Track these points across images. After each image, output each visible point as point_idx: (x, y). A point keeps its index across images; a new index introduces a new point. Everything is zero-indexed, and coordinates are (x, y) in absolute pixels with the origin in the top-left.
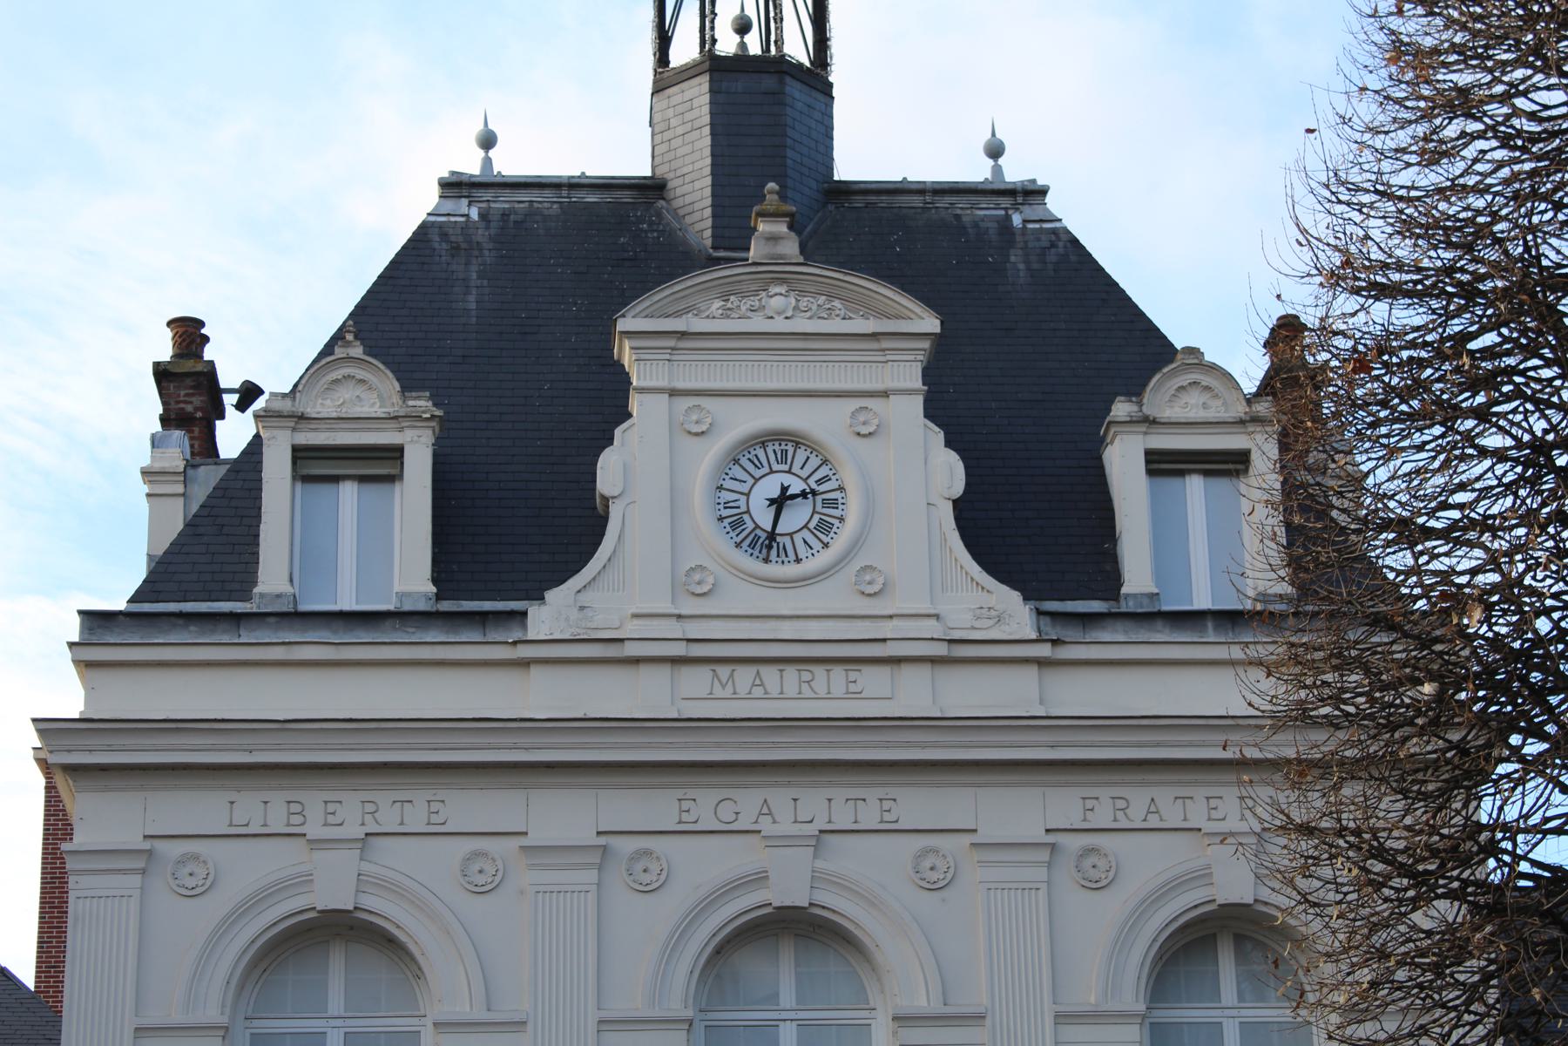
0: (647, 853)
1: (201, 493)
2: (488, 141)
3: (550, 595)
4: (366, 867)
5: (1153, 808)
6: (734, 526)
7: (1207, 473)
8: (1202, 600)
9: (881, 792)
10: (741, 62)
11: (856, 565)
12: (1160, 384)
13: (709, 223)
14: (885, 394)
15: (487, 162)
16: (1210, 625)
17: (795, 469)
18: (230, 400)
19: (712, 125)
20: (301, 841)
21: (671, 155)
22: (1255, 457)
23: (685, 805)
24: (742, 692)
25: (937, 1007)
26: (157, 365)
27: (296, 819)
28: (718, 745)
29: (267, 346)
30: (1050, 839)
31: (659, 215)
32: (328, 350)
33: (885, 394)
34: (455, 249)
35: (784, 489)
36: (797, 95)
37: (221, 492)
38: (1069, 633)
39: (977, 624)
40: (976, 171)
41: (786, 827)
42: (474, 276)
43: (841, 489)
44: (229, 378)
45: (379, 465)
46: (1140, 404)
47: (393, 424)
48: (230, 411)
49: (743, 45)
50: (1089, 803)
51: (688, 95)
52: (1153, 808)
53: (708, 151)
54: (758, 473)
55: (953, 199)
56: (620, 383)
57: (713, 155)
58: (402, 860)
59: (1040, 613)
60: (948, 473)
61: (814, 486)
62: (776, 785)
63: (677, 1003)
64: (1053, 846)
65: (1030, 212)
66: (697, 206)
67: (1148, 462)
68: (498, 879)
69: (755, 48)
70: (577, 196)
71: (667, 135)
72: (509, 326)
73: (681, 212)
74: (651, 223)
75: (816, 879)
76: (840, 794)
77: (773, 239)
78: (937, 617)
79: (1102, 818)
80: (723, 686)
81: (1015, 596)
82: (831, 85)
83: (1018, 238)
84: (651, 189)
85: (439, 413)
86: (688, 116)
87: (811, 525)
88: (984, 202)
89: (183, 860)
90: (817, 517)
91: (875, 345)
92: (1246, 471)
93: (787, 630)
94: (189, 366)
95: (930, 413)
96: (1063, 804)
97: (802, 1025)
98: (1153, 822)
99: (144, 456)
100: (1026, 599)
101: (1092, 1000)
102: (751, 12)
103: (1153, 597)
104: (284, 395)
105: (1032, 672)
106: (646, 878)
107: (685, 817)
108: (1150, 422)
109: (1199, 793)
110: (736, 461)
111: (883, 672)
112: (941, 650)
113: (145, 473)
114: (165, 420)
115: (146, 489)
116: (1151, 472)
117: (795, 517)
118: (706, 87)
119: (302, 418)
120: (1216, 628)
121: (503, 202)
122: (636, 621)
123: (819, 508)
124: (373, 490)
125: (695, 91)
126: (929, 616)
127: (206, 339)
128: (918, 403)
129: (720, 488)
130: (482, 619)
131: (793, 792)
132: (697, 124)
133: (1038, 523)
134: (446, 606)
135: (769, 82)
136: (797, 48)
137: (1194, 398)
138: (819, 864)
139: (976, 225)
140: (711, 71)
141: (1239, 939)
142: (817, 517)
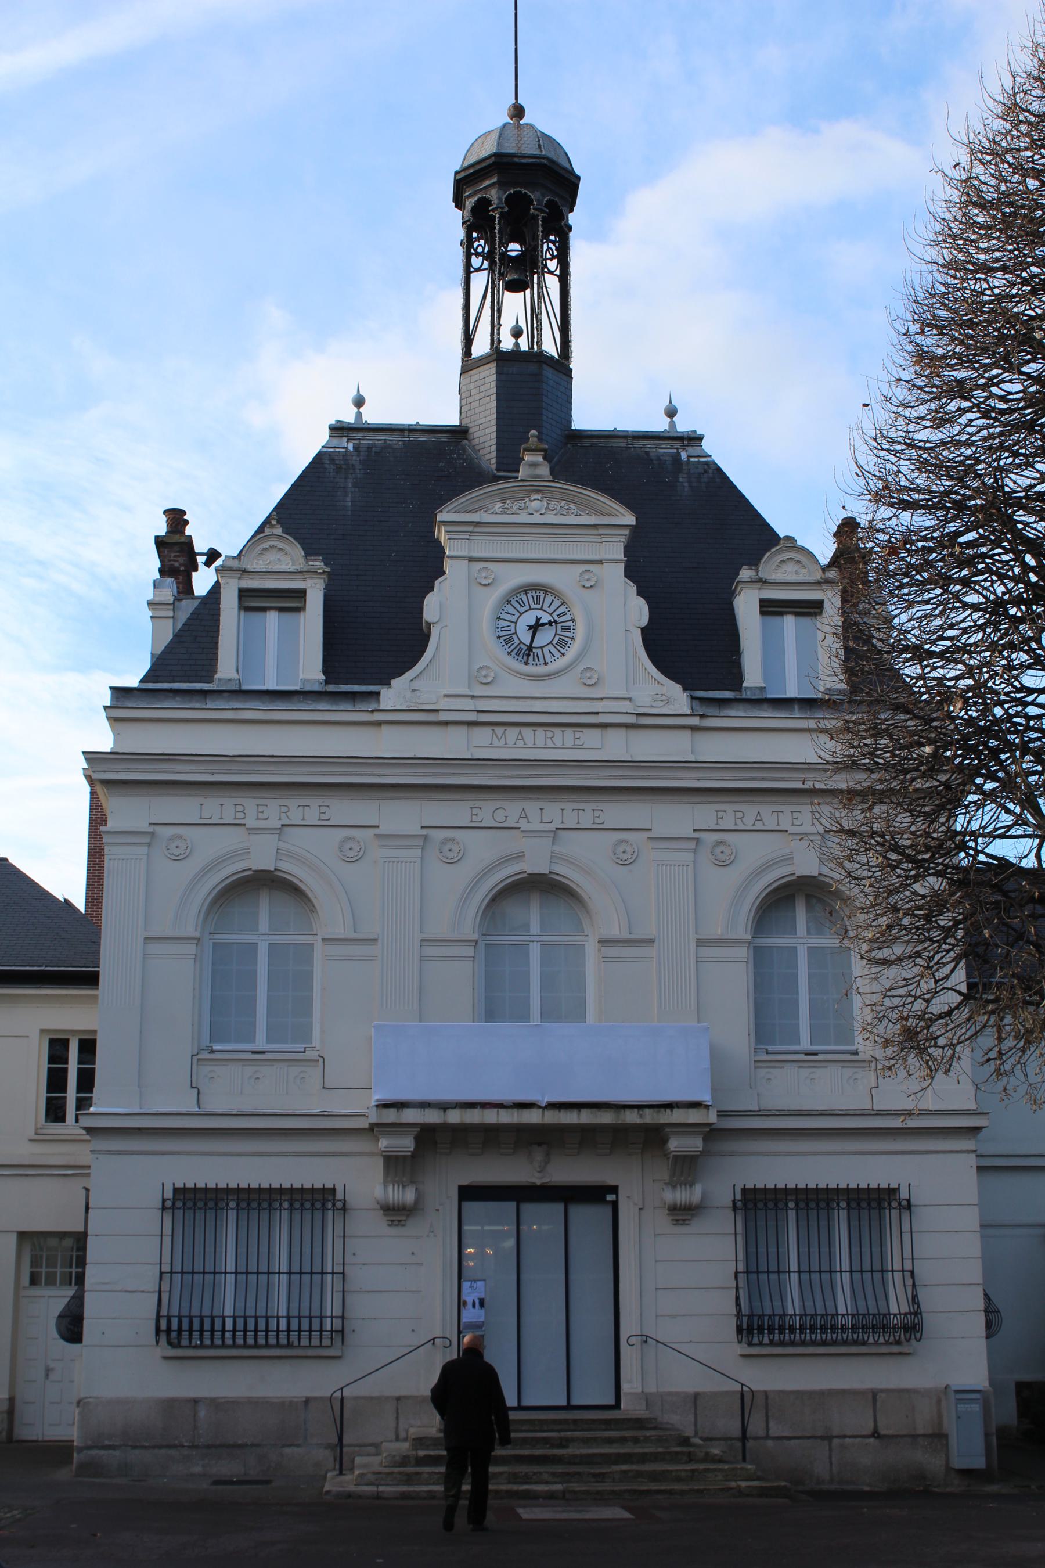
0: (451, 840)
1: (183, 616)
2: (359, 402)
3: (394, 682)
4: (281, 845)
5: (759, 818)
6: (507, 642)
7: (797, 614)
8: (792, 692)
9: (594, 805)
10: (516, 354)
11: (581, 667)
12: (769, 558)
13: (494, 454)
14: (601, 562)
15: (359, 415)
16: (796, 707)
17: (545, 608)
18: (201, 559)
19: (497, 394)
20: (242, 828)
21: (472, 412)
22: (826, 605)
23: (475, 811)
24: (510, 743)
25: (626, 936)
26: (157, 538)
27: (240, 815)
28: (496, 775)
29: (224, 528)
30: (696, 835)
31: (464, 450)
32: (260, 530)
33: (601, 562)
34: (339, 469)
35: (538, 620)
36: (550, 376)
37: (195, 615)
38: (710, 711)
39: (654, 704)
40: (659, 424)
41: (536, 826)
42: (350, 485)
43: (573, 620)
44: (200, 546)
45: (291, 601)
46: (757, 571)
47: (300, 576)
48: (201, 567)
49: (517, 344)
50: (720, 814)
51: (482, 375)
52: (759, 818)
53: (494, 410)
54: (522, 610)
55: (645, 442)
56: (439, 552)
57: (497, 413)
58: (304, 842)
59: (693, 698)
60: (639, 611)
61: (556, 618)
63: (469, 929)
64: (698, 840)
65: (692, 451)
66: (487, 444)
67: (761, 606)
68: (361, 854)
69: (524, 346)
70: (413, 437)
71: (469, 400)
72: (371, 518)
73: (477, 448)
74: (459, 454)
75: (554, 857)
76: (569, 806)
77: (534, 465)
78: (630, 699)
79: (728, 823)
81: (678, 688)
82: (571, 370)
83: (684, 467)
84: (459, 433)
85: (328, 569)
86: (483, 388)
87: (554, 642)
88: (664, 444)
89: (172, 839)
90: (557, 637)
91: (595, 532)
92: (821, 613)
93: (538, 706)
94: (176, 538)
95: (629, 574)
96: (704, 814)
97: (544, 944)
98: (759, 826)
99: (149, 594)
100: (685, 689)
101: (719, 932)
102: (522, 324)
103: (762, 689)
104: (234, 558)
105: (688, 733)
106: (450, 855)
107: (475, 818)
108: (763, 582)
109: (787, 809)
110: (509, 602)
111: (596, 733)
112: (632, 720)
113: (150, 604)
114: (162, 572)
115: (150, 613)
116: (763, 613)
117: (544, 637)
118: (494, 370)
119: (245, 571)
120: (800, 709)
121: (368, 440)
122: (446, 699)
123: (559, 632)
124: (287, 616)
125: (487, 373)
127: (187, 522)
128: (621, 567)
129: (499, 618)
130: (353, 696)
131: (541, 805)
132: (488, 393)
133: (692, 644)
134: (331, 688)
135: (532, 368)
136: (550, 346)
137: (790, 567)
138: (556, 848)
139: (658, 458)
140: (498, 360)
141: (808, 897)
142: (557, 637)
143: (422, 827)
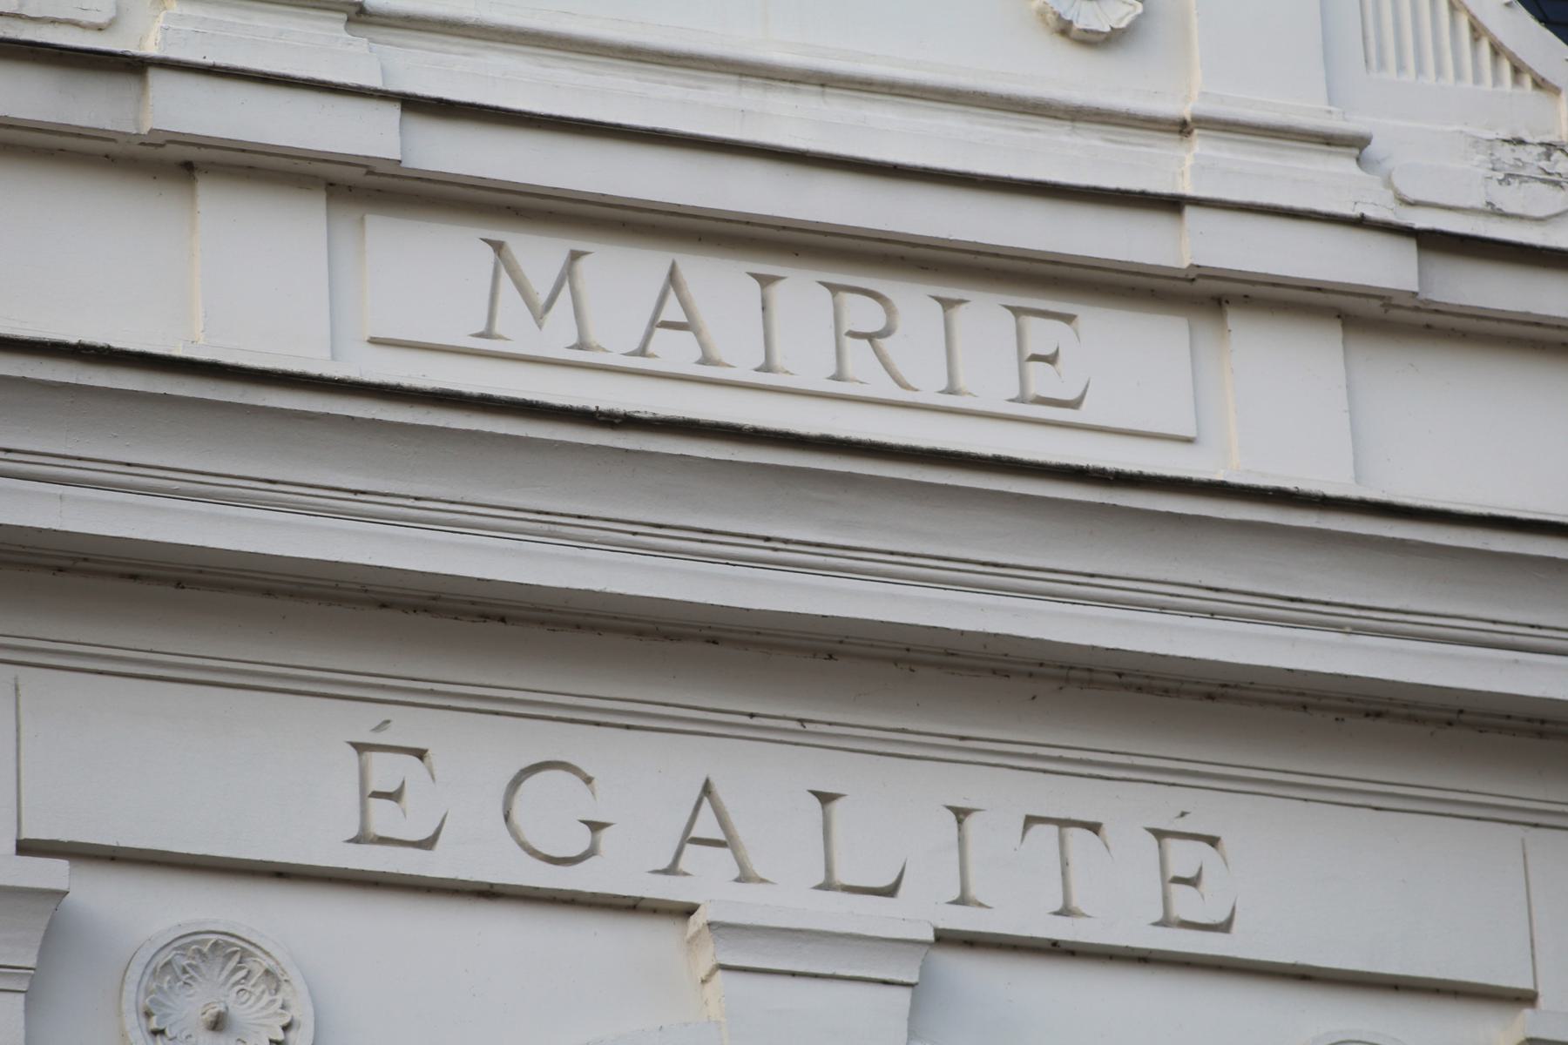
0: (227, 950)
9: (1163, 806)
23: (385, 772)
39: (1510, 198)
41: (791, 898)
62: (752, 729)
76: (1002, 795)
78: (1355, 144)
80: (540, 312)
107: (384, 818)
112: (1389, 268)
126: (1329, 140)
131: (830, 770)
143: (26, 848)
